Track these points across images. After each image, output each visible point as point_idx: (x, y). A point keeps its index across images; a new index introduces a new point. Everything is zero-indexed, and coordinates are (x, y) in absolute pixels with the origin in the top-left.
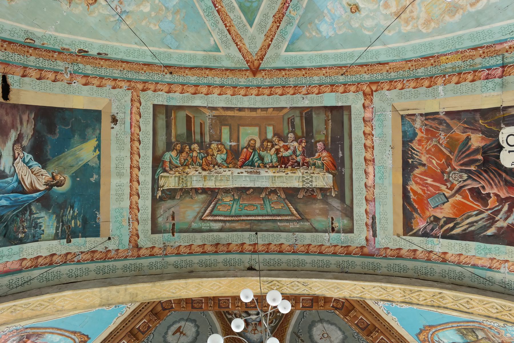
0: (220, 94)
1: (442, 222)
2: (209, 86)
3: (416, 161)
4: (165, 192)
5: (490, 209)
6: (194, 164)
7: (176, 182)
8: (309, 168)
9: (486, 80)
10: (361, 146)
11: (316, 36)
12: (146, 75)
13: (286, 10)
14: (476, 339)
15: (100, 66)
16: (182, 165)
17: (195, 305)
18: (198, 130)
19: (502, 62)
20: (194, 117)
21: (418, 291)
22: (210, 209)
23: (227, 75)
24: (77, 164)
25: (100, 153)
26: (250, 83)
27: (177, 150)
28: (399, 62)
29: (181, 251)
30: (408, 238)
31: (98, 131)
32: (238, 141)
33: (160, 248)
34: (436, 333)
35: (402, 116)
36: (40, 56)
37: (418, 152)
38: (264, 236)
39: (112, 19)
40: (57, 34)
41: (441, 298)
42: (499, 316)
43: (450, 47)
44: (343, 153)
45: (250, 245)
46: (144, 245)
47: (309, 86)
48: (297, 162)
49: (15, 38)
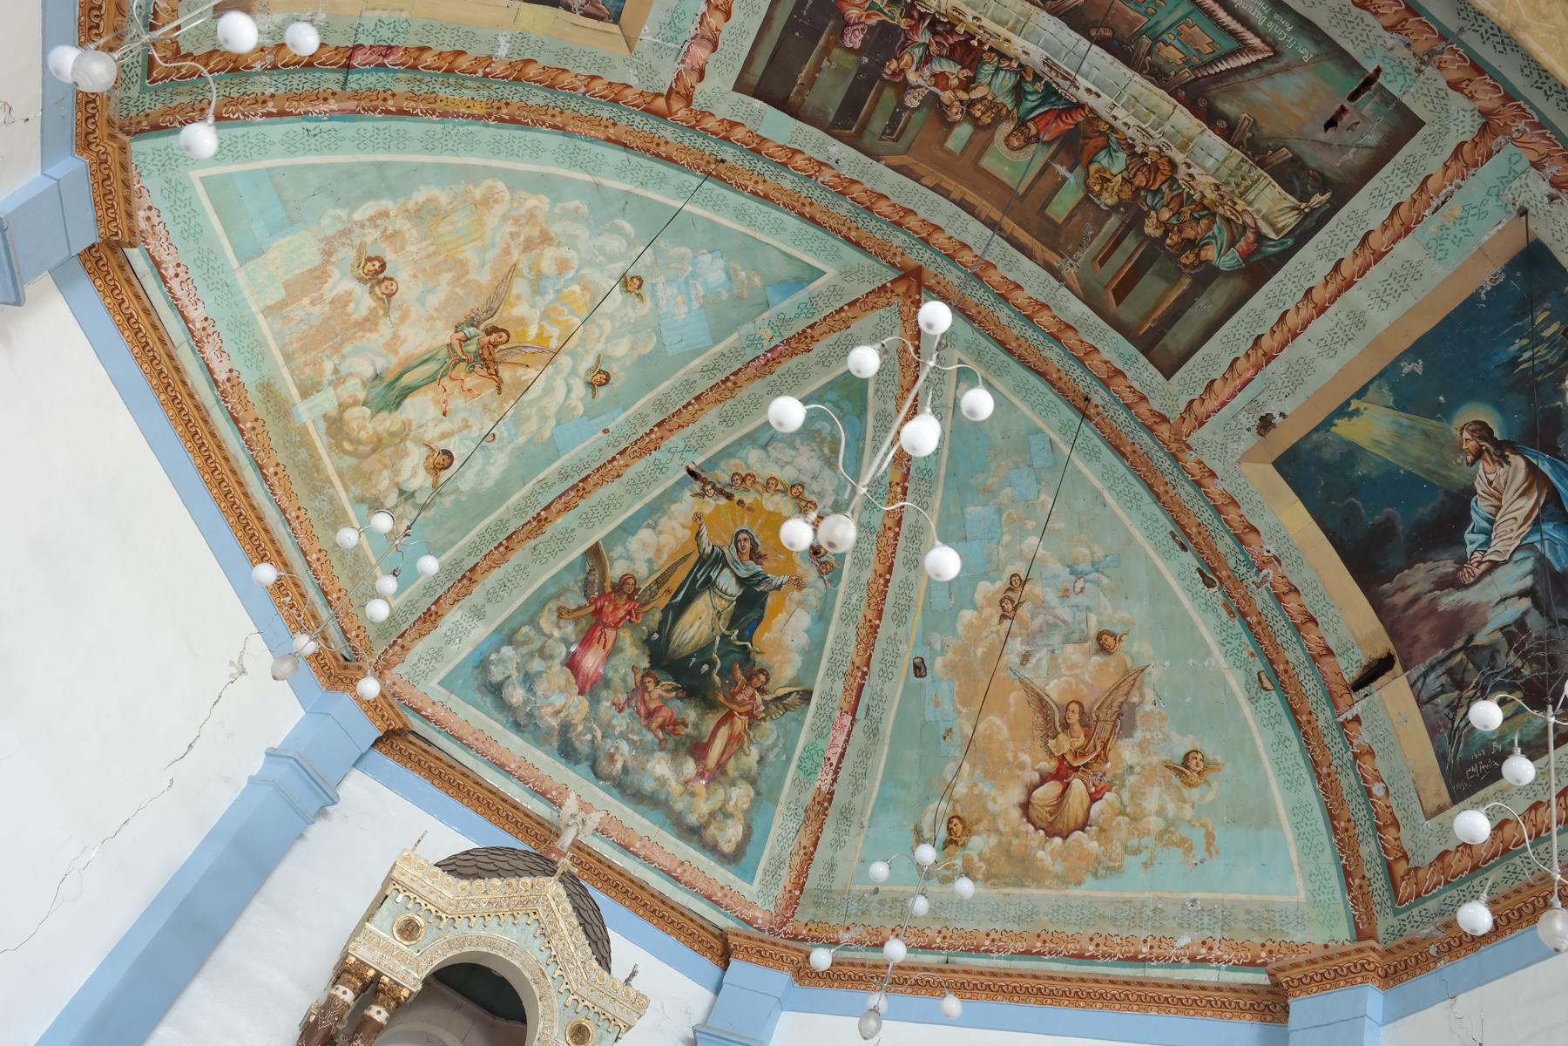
0: (1018, 287)
7: (1257, 191)
13: (777, 346)
15: (1202, 530)
16: (1214, 214)
18: (1118, 258)
20: (1106, 287)
24: (1413, 427)
25: (1352, 397)
27: (1198, 255)
29: (1396, 12)
31: (1315, 437)
32: (1046, 168)
33: (1439, 67)
35: (616, 19)
36: (1276, 646)
39: (1105, 581)
40: (1215, 648)
43: (455, 131)
46: (1468, 115)
47: (810, 176)
48: (934, 33)
49: (1279, 708)
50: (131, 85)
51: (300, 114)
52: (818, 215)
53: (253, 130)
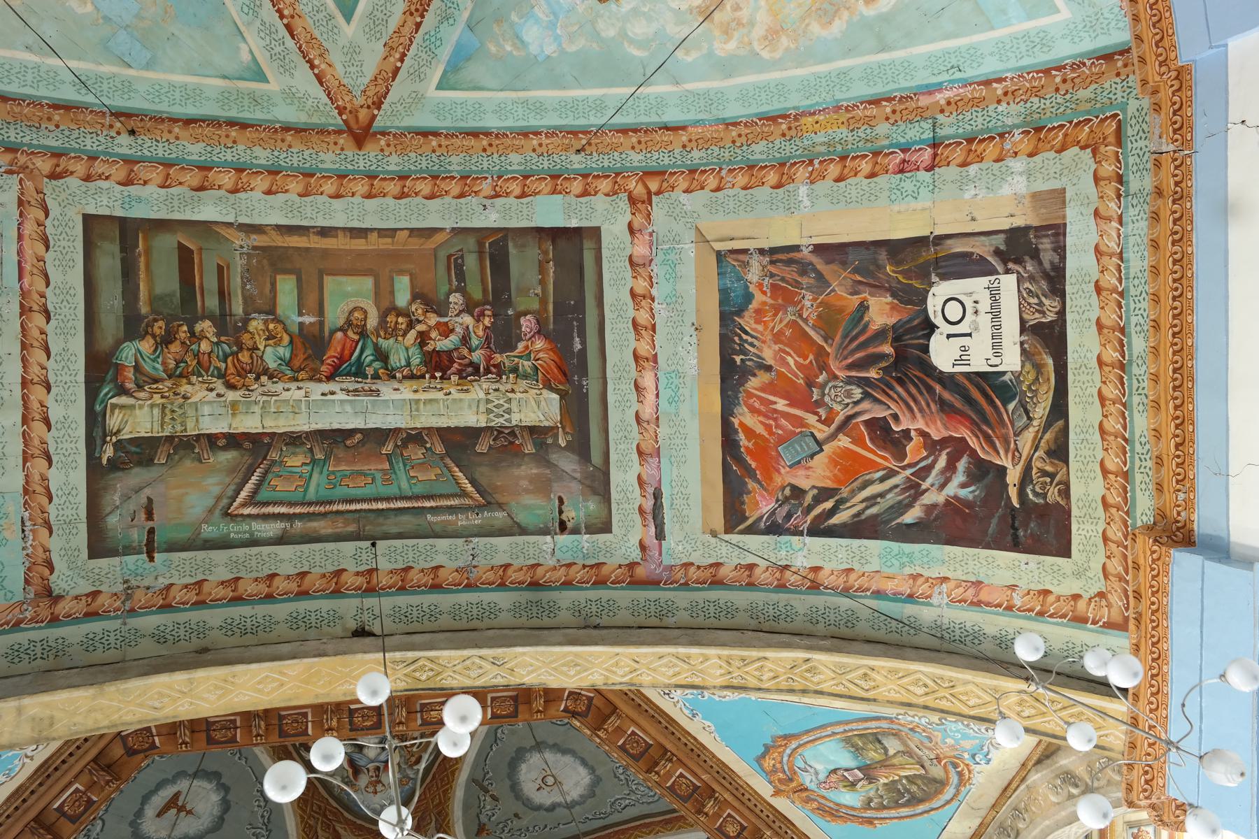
0: (269, 192)
1: (808, 499)
2: (240, 170)
3: (750, 360)
4: (125, 447)
5: (910, 466)
6: (203, 373)
7: (156, 419)
8: (501, 378)
9: (899, 176)
10: (625, 325)
11: (514, 53)
12: (61, 136)
14: (884, 757)
16: (170, 377)
17: (218, 736)
18: (211, 283)
19: (931, 135)
20: (200, 249)
21: (759, 659)
22: (249, 487)
23: (287, 143)
26: (348, 165)
27: (154, 336)
28: (711, 126)
29: (175, 598)
30: (734, 538)
32: (321, 312)
33: (116, 594)
34: (800, 751)
35: (719, 253)
37: (756, 338)
38: (393, 549)
41: (808, 671)
42: (929, 700)
44: (583, 343)
45: (357, 574)
46: (68, 588)
47: (499, 177)
48: (471, 364)
50: (1137, 114)
51: (970, 85)
52: (472, 142)
53: (1013, 64)
